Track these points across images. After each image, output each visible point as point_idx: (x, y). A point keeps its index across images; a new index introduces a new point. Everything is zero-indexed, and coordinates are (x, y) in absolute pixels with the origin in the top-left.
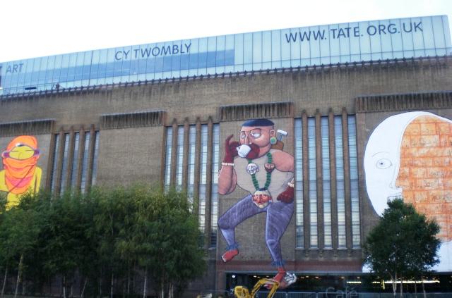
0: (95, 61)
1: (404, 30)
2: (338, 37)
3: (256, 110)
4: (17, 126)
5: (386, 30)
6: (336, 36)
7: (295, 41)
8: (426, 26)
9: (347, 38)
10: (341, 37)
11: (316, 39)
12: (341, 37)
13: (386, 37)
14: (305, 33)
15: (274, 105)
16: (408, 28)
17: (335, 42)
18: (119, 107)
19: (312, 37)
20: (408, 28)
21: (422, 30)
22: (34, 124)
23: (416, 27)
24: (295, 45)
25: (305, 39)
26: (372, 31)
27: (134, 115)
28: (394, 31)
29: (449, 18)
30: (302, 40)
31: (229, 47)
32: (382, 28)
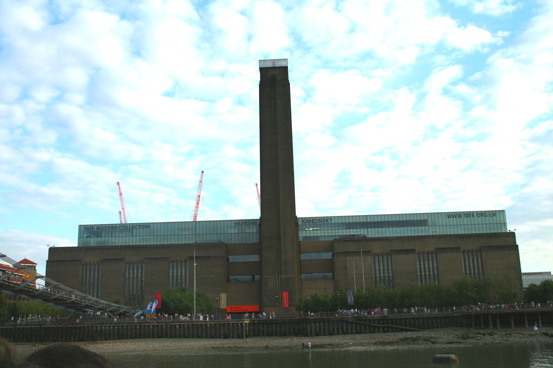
0: (369, 220)
1: (490, 216)
2: (467, 217)
3: (449, 250)
5: (483, 215)
6: (466, 217)
7: (451, 218)
8: (497, 214)
9: (470, 218)
10: (468, 217)
11: (458, 217)
12: (468, 217)
13: (483, 218)
14: (454, 215)
15: (455, 248)
16: (491, 215)
17: (465, 219)
18: (397, 246)
19: (457, 217)
20: (491, 215)
21: (496, 216)
23: (494, 215)
24: (451, 219)
25: (455, 217)
26: (479, 215)
27: (405, 250)
28: (486, 216)
29: (506, 213)
30: (454, 218)
31: (426, 218)
32: (482, 214)
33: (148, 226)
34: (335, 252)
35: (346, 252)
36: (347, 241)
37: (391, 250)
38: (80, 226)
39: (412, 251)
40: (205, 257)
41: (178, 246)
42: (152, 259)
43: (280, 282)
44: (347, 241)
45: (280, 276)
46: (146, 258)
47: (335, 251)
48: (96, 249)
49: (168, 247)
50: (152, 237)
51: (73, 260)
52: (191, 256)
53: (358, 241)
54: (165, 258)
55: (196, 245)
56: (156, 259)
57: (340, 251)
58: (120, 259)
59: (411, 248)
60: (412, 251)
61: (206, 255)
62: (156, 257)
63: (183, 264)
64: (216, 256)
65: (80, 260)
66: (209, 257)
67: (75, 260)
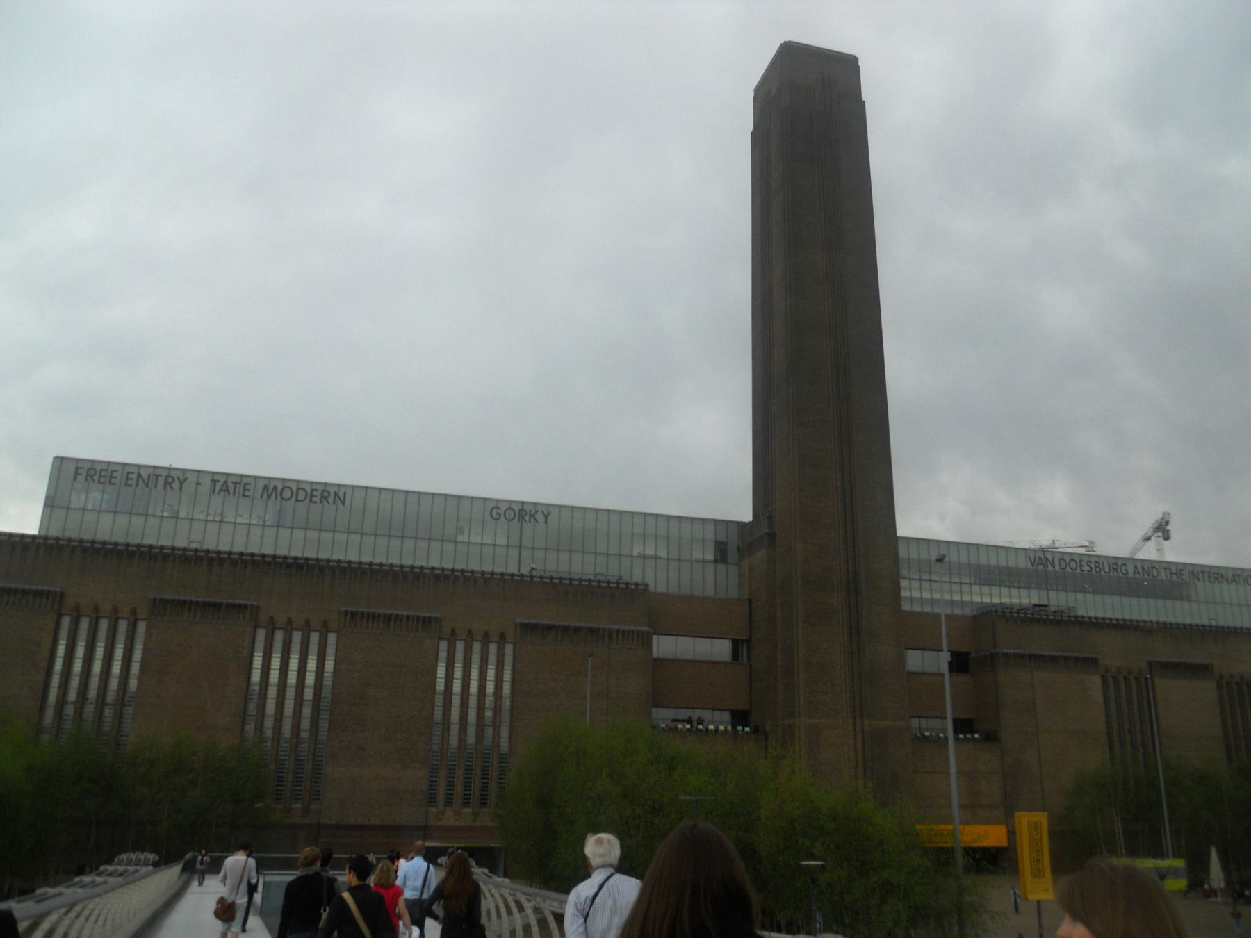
4: (1054, 659)
22: (1077, 659)
33: (341, 495)
35: (1031, 657)
37: (1150, 665)
38: (60, 462)
39: (1199, 670)
40: (577, 630)
41: (476, 580)
42: (373, 617)
43: (859, 745)
44: (1031, 620)
46: (346, 613)
47: (1001, 650)
48: (131, 555)
49: (437, 578)
50: (357, 538)
51: (16, 591)
52: (526, 621)
53: (1059, 623)
54: (426, 621)
55: (546, 583)
56: (388, 618)
57: (1012, 651)
58: (234, 606)
59: (1198, 660)
60: (1199, 670)
61: (582, 625)
62: (388, 612)
63: (493, 648)
64: (618, 631)
65: (49, 593)
67: (24, 592)
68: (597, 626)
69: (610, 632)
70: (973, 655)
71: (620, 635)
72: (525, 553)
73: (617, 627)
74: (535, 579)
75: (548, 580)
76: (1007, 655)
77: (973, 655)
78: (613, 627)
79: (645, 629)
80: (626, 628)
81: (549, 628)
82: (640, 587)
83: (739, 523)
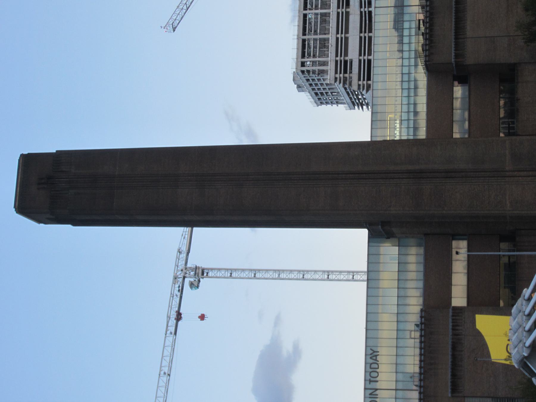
34: (455, 62)
36: (431, 36)
43: (522, 174)
44: (431, 36)
45: (507, 174)
52: (450, 390)
55: (424, 377)
57: (453, 51)
61: (450, 353)
64: (453, 329)
66: (454, 348)
68: (450, 343)
69: (454, 335)
70: (455, 73)
71: (457, 328)
72: (400, 386)
73: (450, 331)
74: (422, 384)
75: (422, 376)
76: (456, 56)
77: (455, 73)
78: (451, 333)
79: (451, 310)
80: (451, 324)
81: (454, 375)
82: (423, 315)
83: (369, 238)
